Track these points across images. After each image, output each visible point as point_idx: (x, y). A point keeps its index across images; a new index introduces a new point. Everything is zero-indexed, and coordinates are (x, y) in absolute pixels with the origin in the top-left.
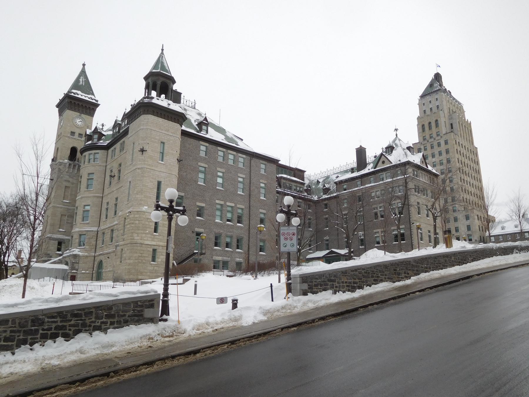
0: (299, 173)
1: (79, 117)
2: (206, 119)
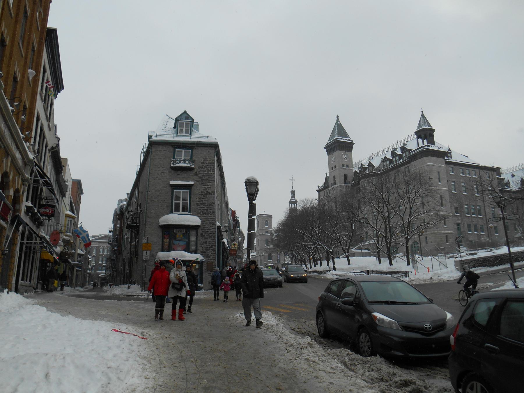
0: (496, 170)
1: (345, 154)
2: (449, 150)
